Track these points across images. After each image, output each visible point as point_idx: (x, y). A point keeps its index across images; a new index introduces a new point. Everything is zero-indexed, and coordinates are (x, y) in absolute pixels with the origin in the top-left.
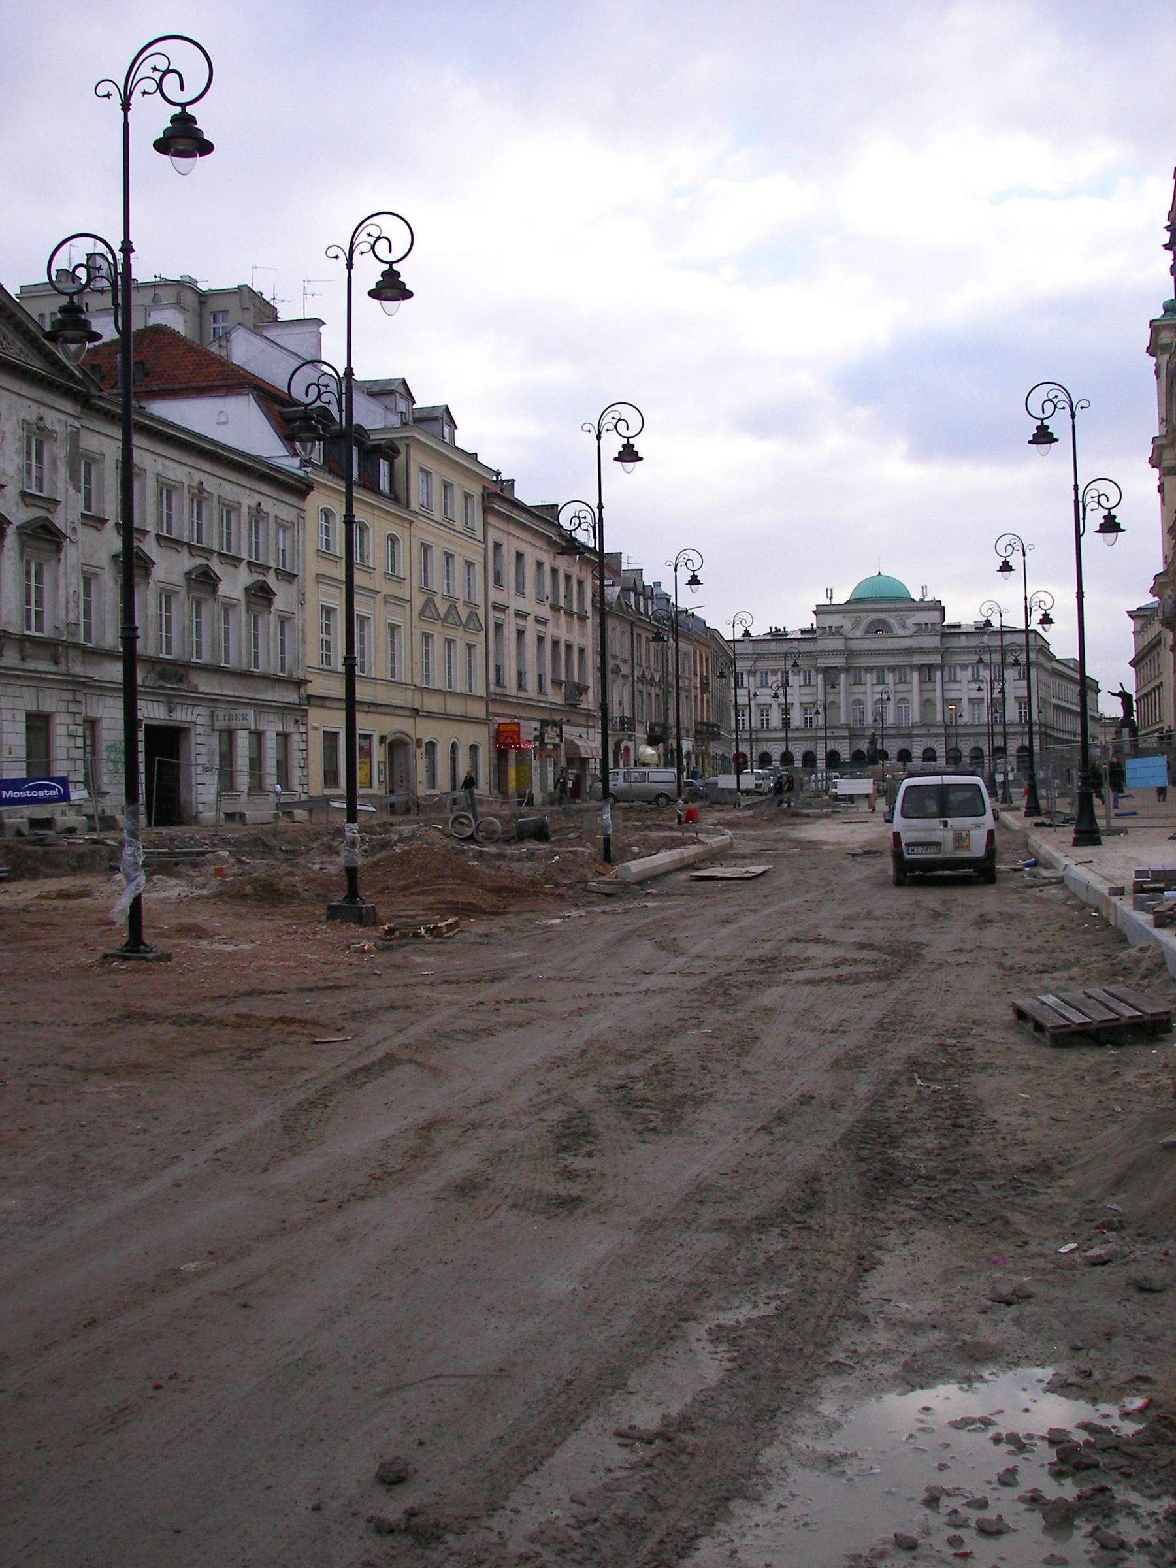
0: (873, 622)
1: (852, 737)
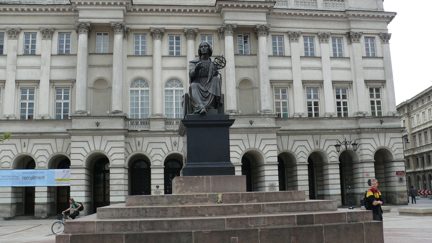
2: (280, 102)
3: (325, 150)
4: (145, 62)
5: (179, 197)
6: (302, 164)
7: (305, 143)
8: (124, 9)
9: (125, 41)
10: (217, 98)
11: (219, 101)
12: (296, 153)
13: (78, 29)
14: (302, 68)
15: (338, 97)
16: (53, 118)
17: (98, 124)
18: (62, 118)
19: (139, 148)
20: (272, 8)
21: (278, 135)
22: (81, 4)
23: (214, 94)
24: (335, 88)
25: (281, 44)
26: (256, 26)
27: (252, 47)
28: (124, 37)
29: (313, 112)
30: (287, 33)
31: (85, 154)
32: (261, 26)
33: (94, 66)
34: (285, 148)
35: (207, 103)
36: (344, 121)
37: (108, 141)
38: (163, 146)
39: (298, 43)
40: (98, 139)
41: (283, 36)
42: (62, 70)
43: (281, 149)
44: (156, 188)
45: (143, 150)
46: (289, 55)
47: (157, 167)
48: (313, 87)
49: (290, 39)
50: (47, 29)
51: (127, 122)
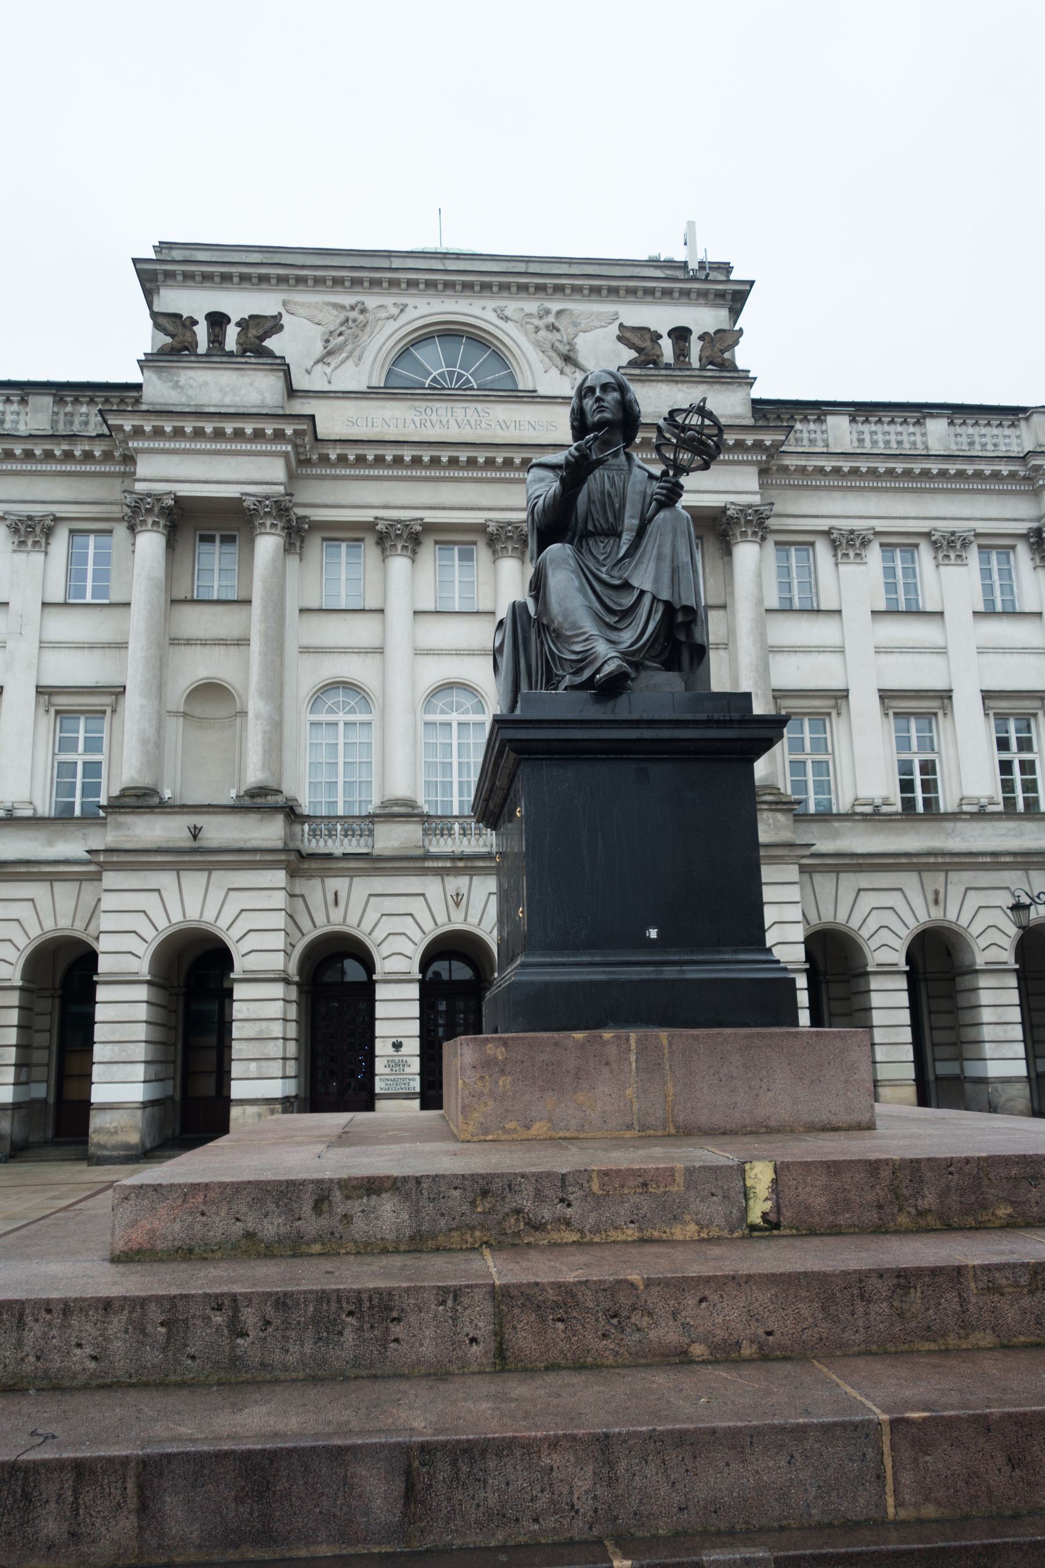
0: (424, 337)
1: (299, 863)
2: (804, 763)
3: (964, 922)
4: (362, 631)
5: (485, 1193)
6: (887, 971)
7: (894, 899)
8: (286, 455)
9: (293, 562)
10: (680, 618)
11: (690, 634)
12: (865, 933)
13: (136, 513)
14: (878, 650)
15: (1003, 744)
16: (46, 815)
17: (195, 833)
18: (77, 812)
19: (337, 915)
20: (777, 445)
21: (803, 869)
22: (144, 432)
23: (665, 596)
24: (991, 713)
25: (811, 571)
26: (724, 509)
27: (711, 582)
28: (289, 548)
29: (919, 794)
30: (827, 533)
31: (149, 933)
32: (743, 509)
33: (189, 642)
34: (827, 916)
35: (627, 637)
36: (1028, 826)
37: (230, 889)
38: (416, 906)
39: (863, 568)
40: (194, 882)
41: (812, 544)
42: (79, 653)
43: (814, 920)
44: (391, 1051)
45: (349, 921)
46: (834, 607)
47: (395, 977)
48: (916, 708)
49: (835, 555)
50: (30, 518)
51: (297, 828)
